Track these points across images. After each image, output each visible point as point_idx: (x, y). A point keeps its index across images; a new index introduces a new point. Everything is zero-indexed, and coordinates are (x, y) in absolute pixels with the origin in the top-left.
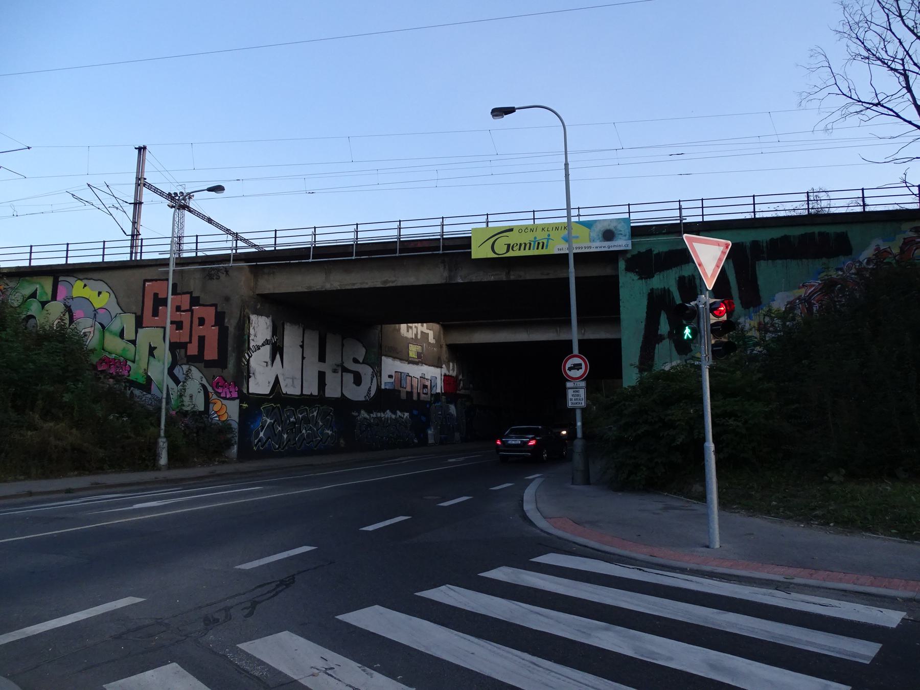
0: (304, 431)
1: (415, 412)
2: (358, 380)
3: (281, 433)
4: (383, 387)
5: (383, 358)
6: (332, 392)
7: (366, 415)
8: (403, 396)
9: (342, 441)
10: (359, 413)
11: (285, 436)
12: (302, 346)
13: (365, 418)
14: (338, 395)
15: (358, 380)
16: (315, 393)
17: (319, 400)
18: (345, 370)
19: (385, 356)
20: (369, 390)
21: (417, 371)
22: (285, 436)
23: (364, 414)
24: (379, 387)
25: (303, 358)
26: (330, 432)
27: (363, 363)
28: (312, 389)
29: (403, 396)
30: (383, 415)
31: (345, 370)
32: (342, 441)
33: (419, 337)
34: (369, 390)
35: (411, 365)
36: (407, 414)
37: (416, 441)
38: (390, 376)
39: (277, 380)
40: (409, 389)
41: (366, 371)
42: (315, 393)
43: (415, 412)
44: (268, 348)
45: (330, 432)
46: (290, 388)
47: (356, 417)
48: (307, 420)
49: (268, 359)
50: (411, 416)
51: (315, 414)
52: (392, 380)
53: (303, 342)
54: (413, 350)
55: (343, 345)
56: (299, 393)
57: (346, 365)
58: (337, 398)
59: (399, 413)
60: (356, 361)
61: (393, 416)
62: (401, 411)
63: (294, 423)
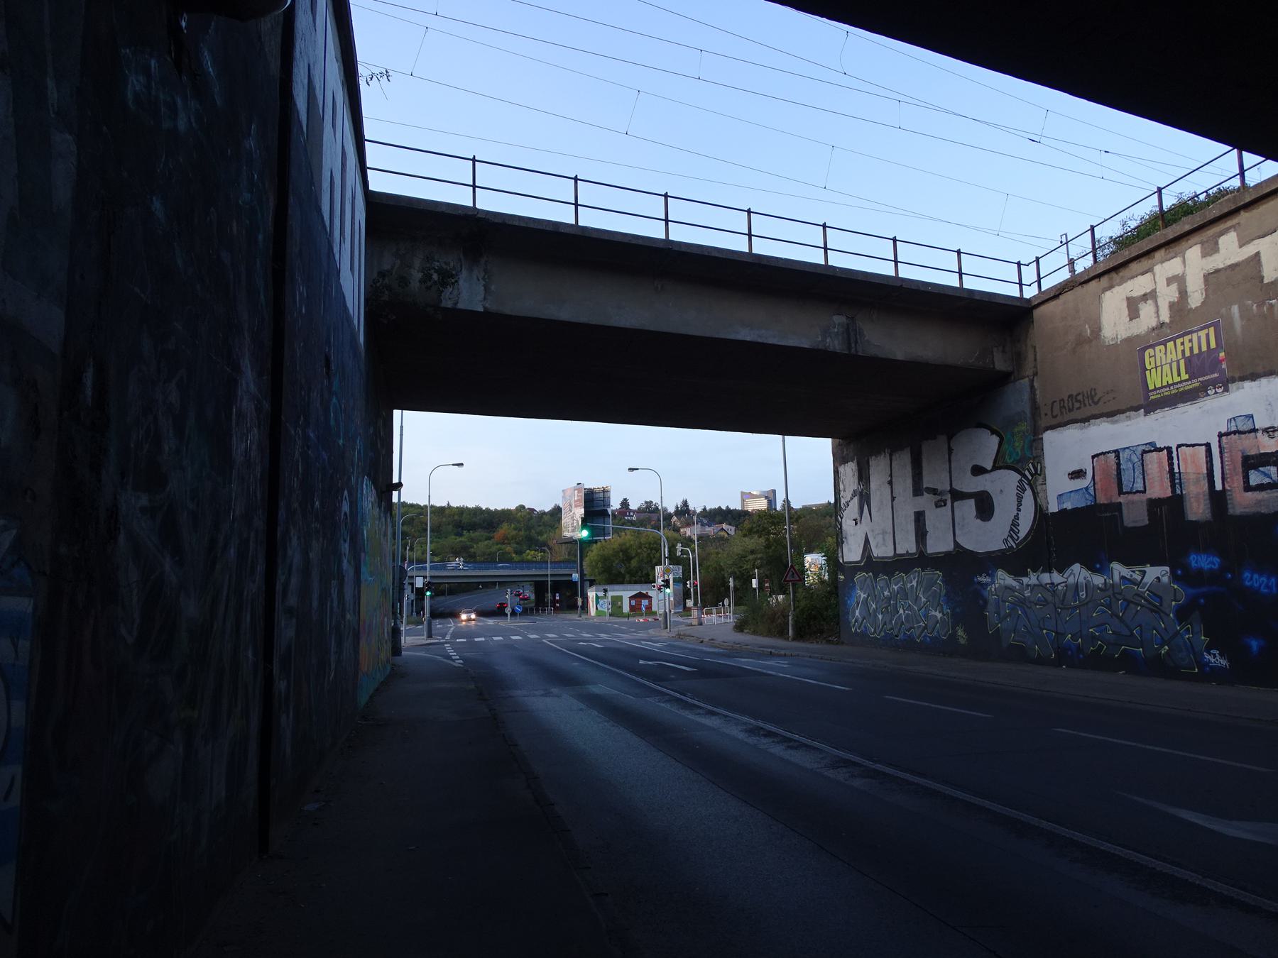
0: (901, 611)
1: (1203, 561)
2: (985, 507)
3: (875, 611)
4: (1053, 508)
5: (1048, 437)
6: (939, 544)
7: (1009, 580)
8: (1135, 516)
9: (960, 632)
10: (992, 575)
11: (880, 617)
12: (890, 483)
13: (1008, 588)
14: (950, 547)
15: (985, 507)
16: (913, 549)
17: (921, 560)
18: (957, 496)
19: (1052, 428)
20: (1015, 524)
21: (1195, 425)
22: (880, 617)
23: (1004, 578)
24: (1040, 512)
25: (893, 499)
26: (939, 615)
27: (995, 468)
28: (908, 545)
29: (1135, 516)
30: (1057, 577)
31: (957, 496)
32: (960, 632)
33: (1196, 299)
34: (1015, 524)
35: (1158, 415)
36: (1155, 573)
37: (1216, 659)
38: (1077, 474)
39: (867, 541)
40: (1159, 488)
41: (1003, 485)
42: (913, 549)
43: (1203, 561)
44: (856, 500)
45: (939, 615)
46: (882, 550)
47: (987, 584)
48: (904, 593)
49: (857, 516)
50: (1183, 575)
51: (914, 583)
52: (1086, 482)
53: (891, 475)
54: (1164, 367)
55: (950, 451)
56: (891, 554)
57: (957, 486)
58: (947, 554)
59: (1118, 569)
60: (978, 471)
61: (1098, 580)
62: (1127, 563)
63: (889, 599)
